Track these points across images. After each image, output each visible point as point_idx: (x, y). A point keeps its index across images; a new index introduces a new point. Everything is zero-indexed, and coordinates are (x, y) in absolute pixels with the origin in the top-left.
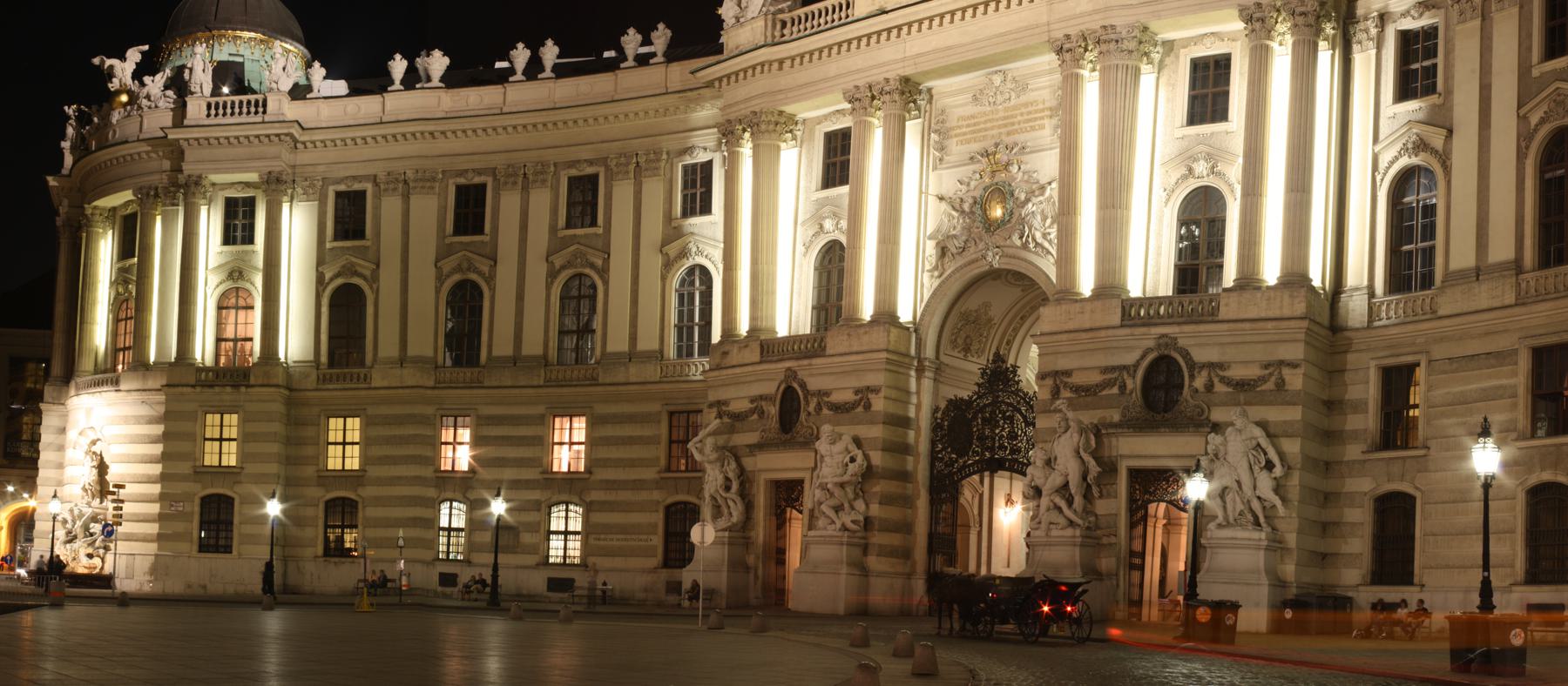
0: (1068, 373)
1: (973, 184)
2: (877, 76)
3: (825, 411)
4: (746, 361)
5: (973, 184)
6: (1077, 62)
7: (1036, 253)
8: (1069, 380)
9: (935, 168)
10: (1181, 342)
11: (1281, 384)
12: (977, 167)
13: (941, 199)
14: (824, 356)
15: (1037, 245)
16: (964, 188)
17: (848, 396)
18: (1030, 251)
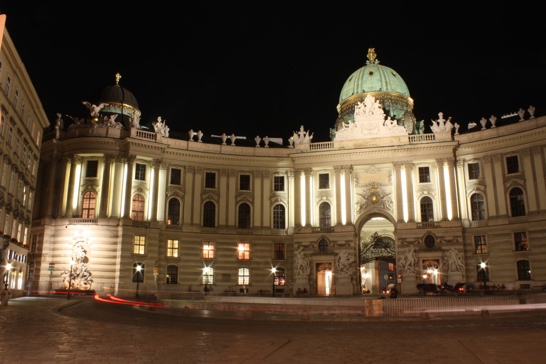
0: (406, 239)
1: (367, 192)
2: (344, 164)
3: (336, 246)
4: (307, 232)
5: (367, 192)
6: (400, 167)
7: (387, 210)
8: (406, 240)
9: (356, 187)
10: (433, 232)
11: (457, 241)
12: (368, 188)
13: (359, 194)
14: (334, 232)
15: (387, 207)
16: (365, 193)
17: (343, 242)
18: (385, 209)
